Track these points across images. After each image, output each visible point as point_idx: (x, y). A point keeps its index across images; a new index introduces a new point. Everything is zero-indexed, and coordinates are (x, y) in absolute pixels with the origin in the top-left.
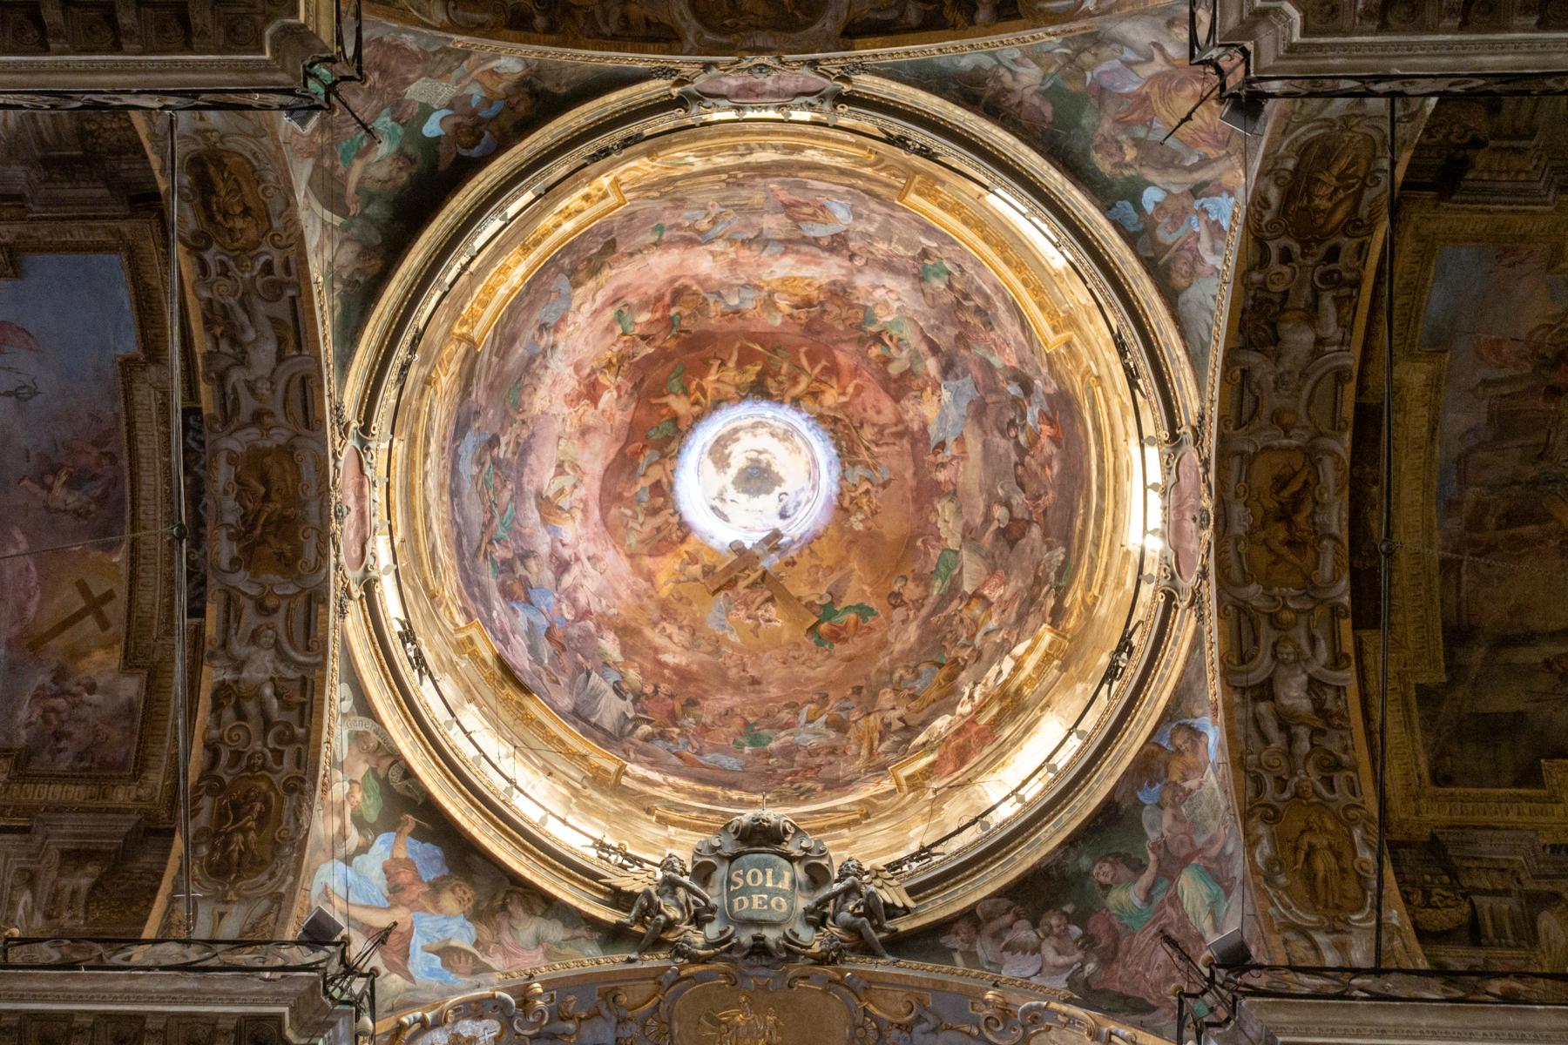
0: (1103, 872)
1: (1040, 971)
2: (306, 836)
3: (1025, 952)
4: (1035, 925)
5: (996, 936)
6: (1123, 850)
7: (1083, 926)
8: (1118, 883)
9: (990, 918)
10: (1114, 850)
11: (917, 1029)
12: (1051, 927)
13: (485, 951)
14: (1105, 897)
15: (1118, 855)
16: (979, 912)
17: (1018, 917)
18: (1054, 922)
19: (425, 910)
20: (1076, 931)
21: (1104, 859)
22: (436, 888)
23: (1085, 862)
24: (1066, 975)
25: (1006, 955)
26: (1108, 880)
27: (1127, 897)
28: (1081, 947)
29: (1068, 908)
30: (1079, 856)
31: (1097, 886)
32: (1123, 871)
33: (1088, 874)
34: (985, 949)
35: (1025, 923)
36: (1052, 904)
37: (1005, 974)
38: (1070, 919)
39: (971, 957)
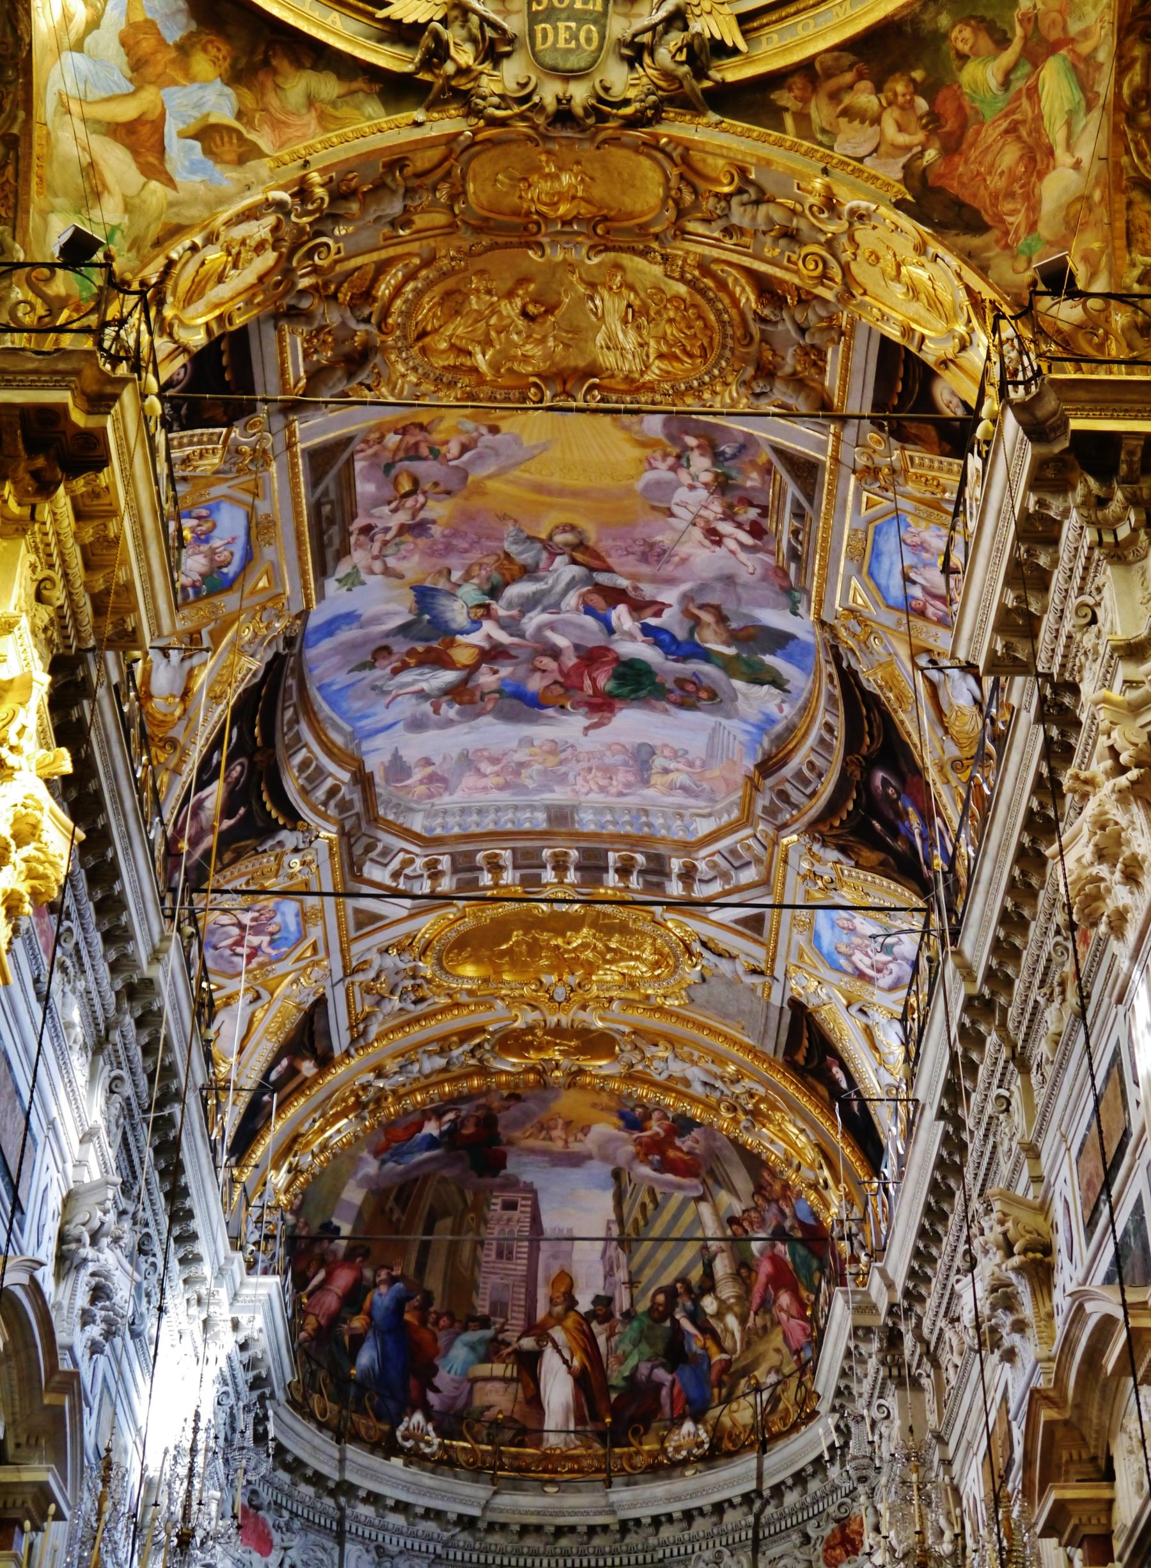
0: (963, 37)
1: (876, 150)
2: (30, 52)
3: (863, 122)
4: (878, 89)
5: (835, 96)
6: (989, 15)
7: (931, 102)
8: (977, 55)
9: (829, 75)
10: (980, 12)
11: (735, 201)
12: (895, 94)
13: (250, 124)
14: (960, 69)
15: (982, 20)
16: (817, 66)
17: (860, 77)
18: (900, 88)
19: (174, 83)
20: (922, 104)
21: (966, 21)
22: (184, 49)
23: (944, 21)
24: (903, 160)
25: (843, 121)
26: (965, 49)
27: (982, 76)
28: (924, 127)
29: (918, 75)
30: (939, 13)
31: (952, 54)
32: (985, 42)
33: (946, 36)
34: (820, 112)
35: (866, 84)
36: (901, 66)
37: (838, 154)
38: (919, 89)
39: (802, 118)
